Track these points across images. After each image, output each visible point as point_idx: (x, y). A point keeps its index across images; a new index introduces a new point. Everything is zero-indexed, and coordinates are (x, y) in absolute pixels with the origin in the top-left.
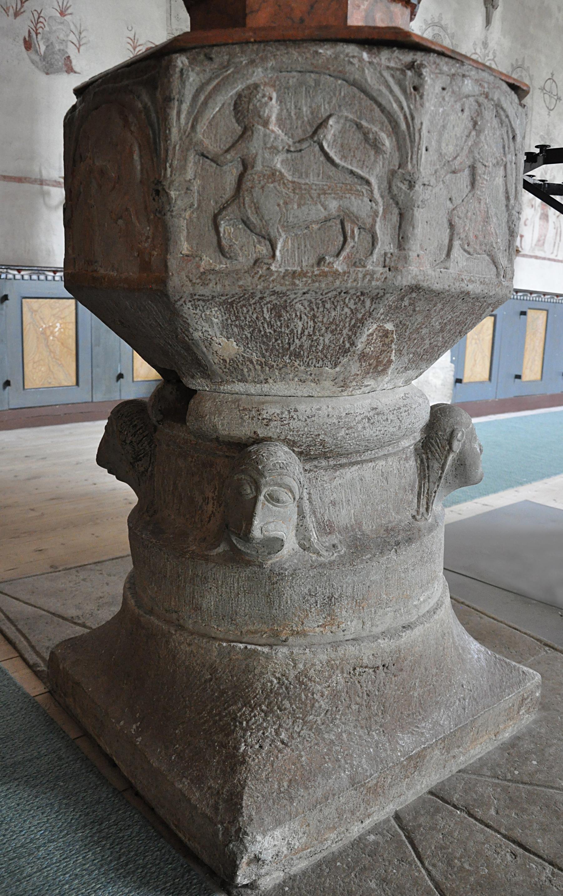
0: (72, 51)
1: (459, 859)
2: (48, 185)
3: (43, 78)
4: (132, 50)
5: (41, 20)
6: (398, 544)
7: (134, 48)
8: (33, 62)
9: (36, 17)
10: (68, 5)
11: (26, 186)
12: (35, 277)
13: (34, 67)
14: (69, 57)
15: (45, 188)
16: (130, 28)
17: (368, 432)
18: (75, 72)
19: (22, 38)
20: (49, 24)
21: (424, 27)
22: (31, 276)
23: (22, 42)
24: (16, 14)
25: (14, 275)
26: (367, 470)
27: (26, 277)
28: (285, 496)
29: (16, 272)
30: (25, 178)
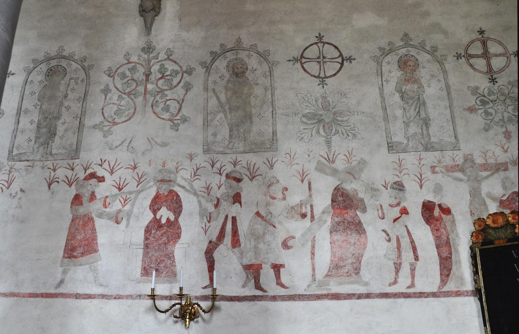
21: (32, 66)
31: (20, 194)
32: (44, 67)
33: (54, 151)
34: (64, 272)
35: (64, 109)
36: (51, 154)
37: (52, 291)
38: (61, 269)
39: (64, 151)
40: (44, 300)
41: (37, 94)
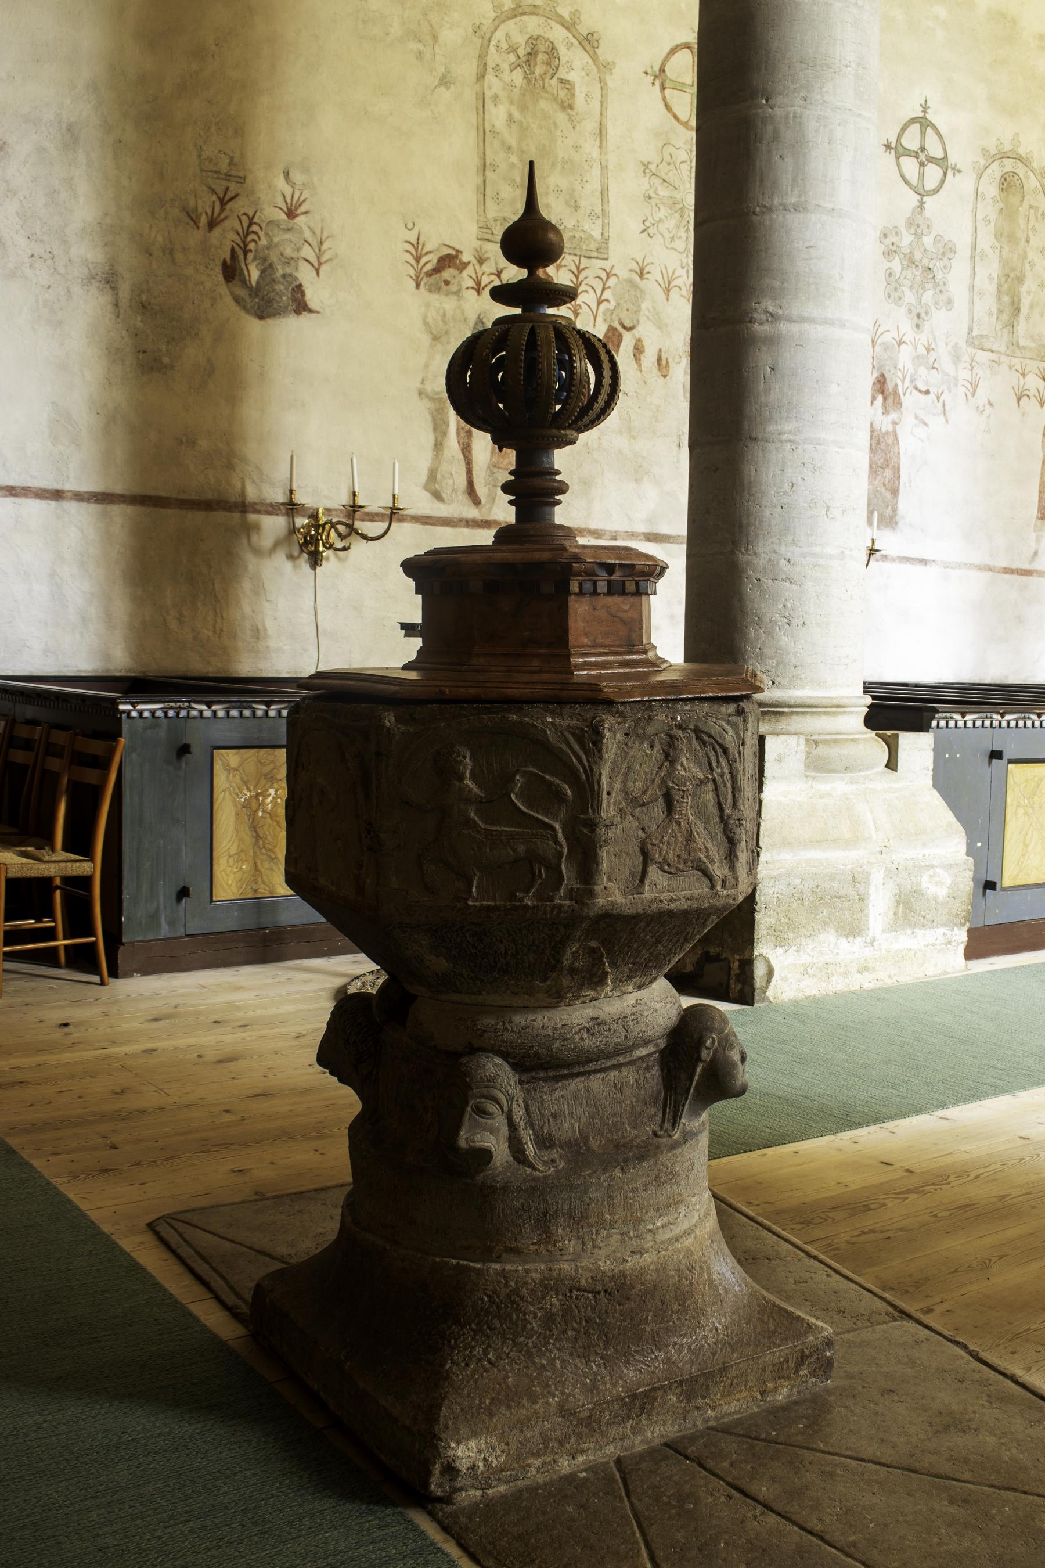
0: (305, 275)
1: (668, 1497)
2: (259, 512)
3: (254, 326)
4: (413, 262)
5: (255, 228)
6: (626, 1161)
7: (418, 259)
8: (237, 300)
9: (245, 225)
10: (302, 199)
11: (220, 516)
12: (234, 713)
13: (238, 308)
14: (300, 285)
15: (252, 517)
16: (410, 226)
17: (588, 1043)
18: (311, 311)
19: (219, 263)
20: (267, 234)
21: (983, 162)
22: (228, 712)
23: (218, 269)
24: (212, 224)
25: (201, 712)
26: (596, 1082)
27: (221, 714)
28: (492, 1108)
29: (204, 707)
30: (218, 503)
31: (988, 410)
32: (995, 171)
33: (1022, 343)
34: (1038, 540)
35: (1027, 266)
36: (1018, 346)
37: (1026, 566)
38: (1034, 535)
39: (1033, 345)
40: (1020, 578)
41: (993, 224)
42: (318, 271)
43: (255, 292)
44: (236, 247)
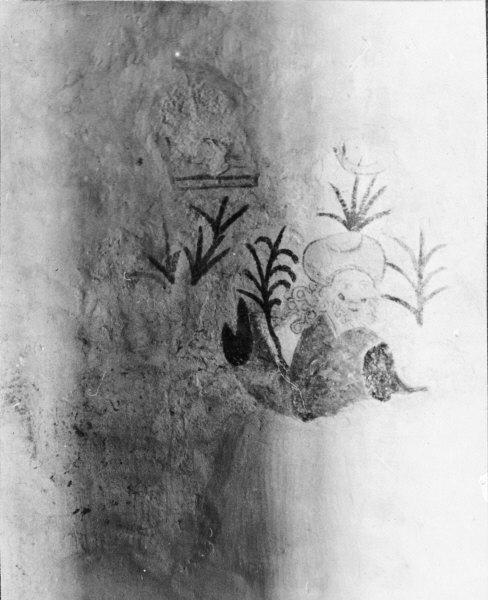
9: (264, 259)
19: (216, 335)
24: (198, 269)
42: (418, 315)
43: (294, 371)
44: (247, 300)
